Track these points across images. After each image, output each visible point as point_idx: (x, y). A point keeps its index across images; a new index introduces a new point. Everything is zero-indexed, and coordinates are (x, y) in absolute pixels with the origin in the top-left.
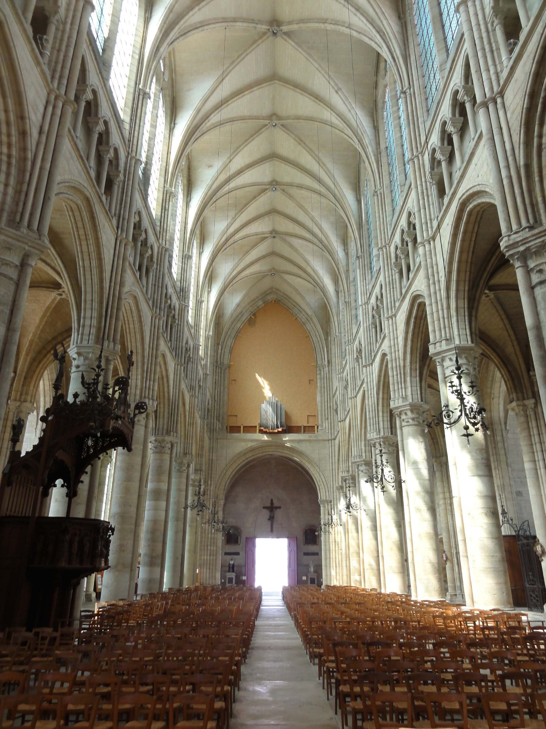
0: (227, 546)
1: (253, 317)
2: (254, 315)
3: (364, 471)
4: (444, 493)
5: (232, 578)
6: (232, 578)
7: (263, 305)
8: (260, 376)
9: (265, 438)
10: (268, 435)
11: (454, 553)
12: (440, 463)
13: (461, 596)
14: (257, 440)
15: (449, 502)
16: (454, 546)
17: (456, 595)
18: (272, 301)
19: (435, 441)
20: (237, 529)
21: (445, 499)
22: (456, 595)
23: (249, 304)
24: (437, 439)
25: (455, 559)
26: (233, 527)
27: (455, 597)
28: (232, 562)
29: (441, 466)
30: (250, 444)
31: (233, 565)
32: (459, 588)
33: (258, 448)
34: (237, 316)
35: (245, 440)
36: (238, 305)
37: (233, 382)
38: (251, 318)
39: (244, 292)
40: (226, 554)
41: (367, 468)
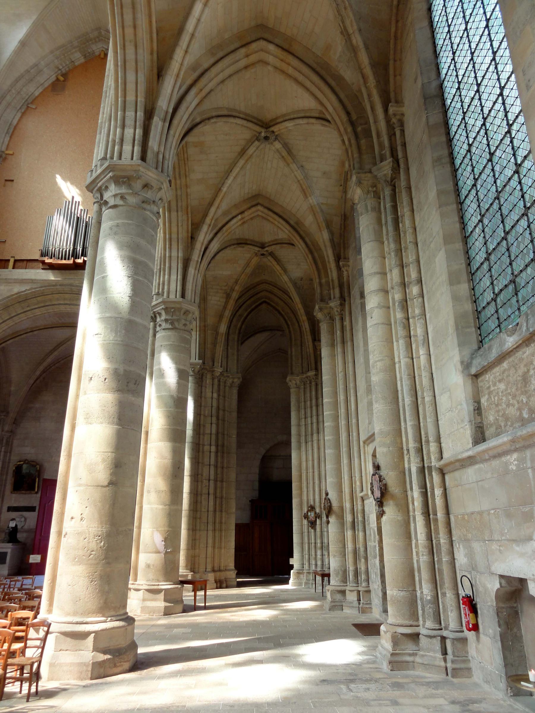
0: (14, 495)
1: (62, 79)
2: (64, 75)
3: (112, 202)
4: (383, 274)
5: (6, 553)
6: (6, 553)
7: (82, 60)
8: (64, 179)
9: (51, 276)
10: (57, 271)
11: (414, 470)
12: (374, 186)
13: (437, 644)
14: (32, 281)
15: (398, 296)
16: (412, 445)
17: (415, 637)
18: (100, 55)
19: (359, 129)
20: (33, 464)
21: (385, 291)
22: (415, 637)
23: (52, 52)
24: (367, 123)
25: (416, 494)
26: (26, 461)
27: (410, 647)
28: (12, 524)
29: (377, 196)
30: (16, 289)
31: (15, 529)
32: (430, 609)
33: (35, 295)
34: (28, 71)
35: (8, 281)
36: (23, 44)
37: (9, 183)
38: (57, 79)
39: (34, 17)
40: (10, 509)
41: (123, 190)
